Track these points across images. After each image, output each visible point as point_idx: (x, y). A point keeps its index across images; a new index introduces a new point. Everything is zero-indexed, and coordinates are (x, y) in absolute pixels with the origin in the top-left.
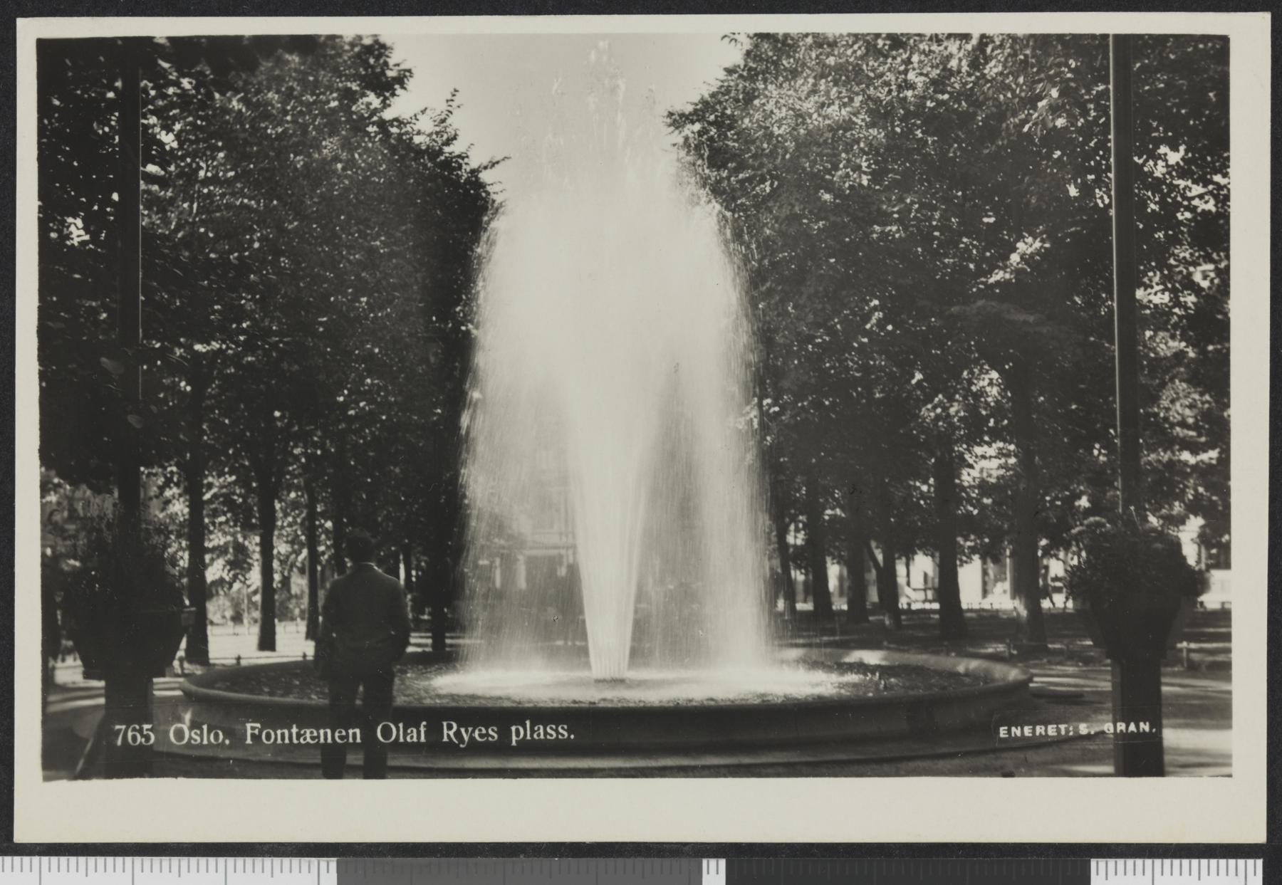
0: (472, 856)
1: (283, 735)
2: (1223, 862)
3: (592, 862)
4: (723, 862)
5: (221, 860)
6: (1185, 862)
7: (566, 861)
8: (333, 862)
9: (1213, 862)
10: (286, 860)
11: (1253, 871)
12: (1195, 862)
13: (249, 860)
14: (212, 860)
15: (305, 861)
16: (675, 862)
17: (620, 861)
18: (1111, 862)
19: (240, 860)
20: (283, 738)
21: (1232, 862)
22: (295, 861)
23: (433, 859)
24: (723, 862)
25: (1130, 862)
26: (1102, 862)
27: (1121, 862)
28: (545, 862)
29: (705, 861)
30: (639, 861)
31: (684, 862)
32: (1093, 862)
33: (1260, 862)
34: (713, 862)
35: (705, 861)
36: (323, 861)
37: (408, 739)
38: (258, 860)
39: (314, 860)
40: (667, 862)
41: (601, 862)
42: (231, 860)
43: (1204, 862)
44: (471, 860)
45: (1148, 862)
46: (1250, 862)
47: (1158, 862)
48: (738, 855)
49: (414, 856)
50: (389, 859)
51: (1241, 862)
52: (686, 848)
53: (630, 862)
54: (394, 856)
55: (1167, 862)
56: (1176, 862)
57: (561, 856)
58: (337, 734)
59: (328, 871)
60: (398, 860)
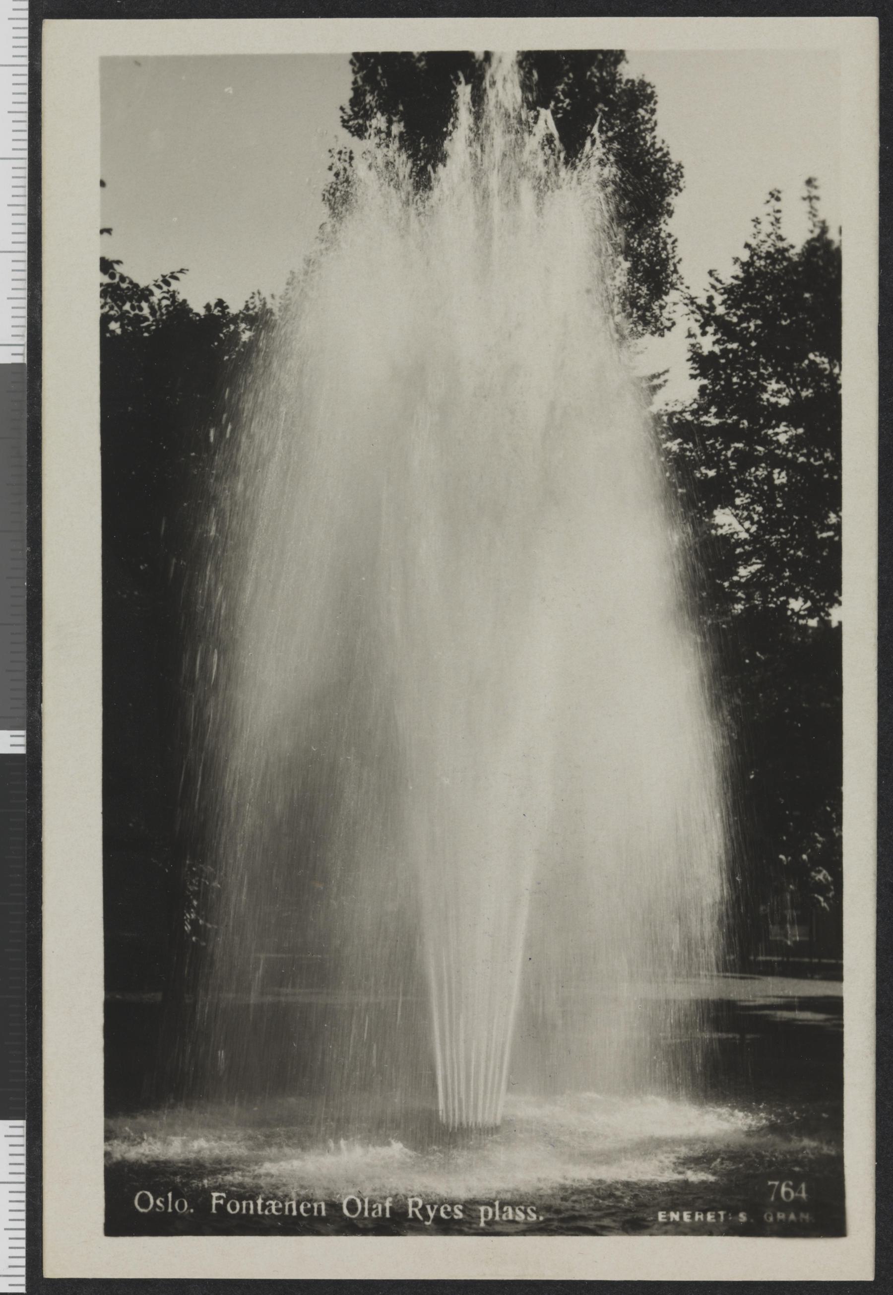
0: (28, 499)
1: (248, 1205)
3: (23, 620)
4: (22, 750)
5: (25, 247)
6: (23, 1215)
7: (24, 593)
8: (22, 359)
9: (23, 1243)
10: (24, 312)
12: (23, 1225)
13: (25, 275)
14: (25, 238)
15: (24, 331)
16: (23, 703)
17: (24, 648)
19: (24, 266)
20: (248, 1209)
21: (23, 1262)
22: (24, 322)
23: (25, 460)
24: (22, 750)
26: (22, 1131)
27: (23, 1150)
29: (23, 733)
30: (24, 667)
31: (23, 712)
32: (22, 1123)
34: (23, 741)
35: (23, 733)
36: (23, 350)
38: (25, 284)
39: (24, 340)
41: (24, 629)
42: (24, 257)
43: (23, 1234)
44: (24, 498)
45: (23, 1178)
46: (23, 1281)
47: (23, 1187)
48: (31, 764)
49: (29, 441)
51: (23, 1271)
52: (36, 714)
53: (23, 657)
55: (23, 1197)
56: (23, 1206)
59: (14, 354)
60: (24, 425)
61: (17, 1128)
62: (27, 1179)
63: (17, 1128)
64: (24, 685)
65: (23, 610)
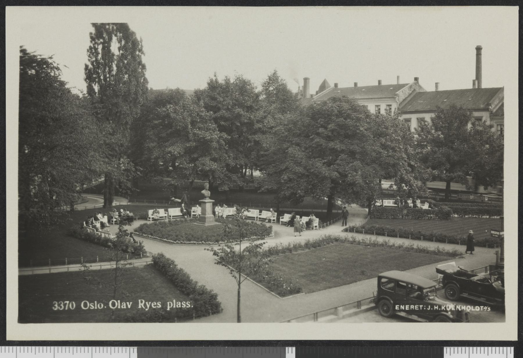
2: (497, 348)
3: (241, 348)
4: (294, 348)
5: (90, 348)
6: (482, 348)
7: (230, 348)
8: (136, 349)
9: (494, 348)
10: (117, 348)
11: (510, 351)
12: (486, 348)
13: (101, 348)
14: (86, 348)
15: (124, 348)
17: (252, 348)
18: (452, 348)
19: (98, 348)
21: (501, 348)
22: (120, 348)
23: (177, 348)
25: (460, 348)
26: (448, 348)
27: (456, 348)
28: (222, 348)
29: (287, 348)
30: (260, 348)
31: (278, 348)
32: (445, 348)
33: (512, 348)
34: (290, 348)
35: (287, 348)
36: (132, 348)
37: (177, 307)
38: (105, 348)
39: (128, 348)
40: (271, 348)
41: (245, 348)
42: (94, 348)
43: (490, 348)
45: (467, 348)
46: (509, 348)
47: (471, 348)
50: (158, 347)
51: (505, 348)
53: (256, 348)
54: (160, 346)
55: (475, 348)
56: (479, 348)
57: (228, 346)
58: (153, 304)
59: (134, 352)
60: (162, 348)
61: (447, 350)
62: (468, 346)
63: (447, 350)
64: (267, 348)
65: (237, 348)
